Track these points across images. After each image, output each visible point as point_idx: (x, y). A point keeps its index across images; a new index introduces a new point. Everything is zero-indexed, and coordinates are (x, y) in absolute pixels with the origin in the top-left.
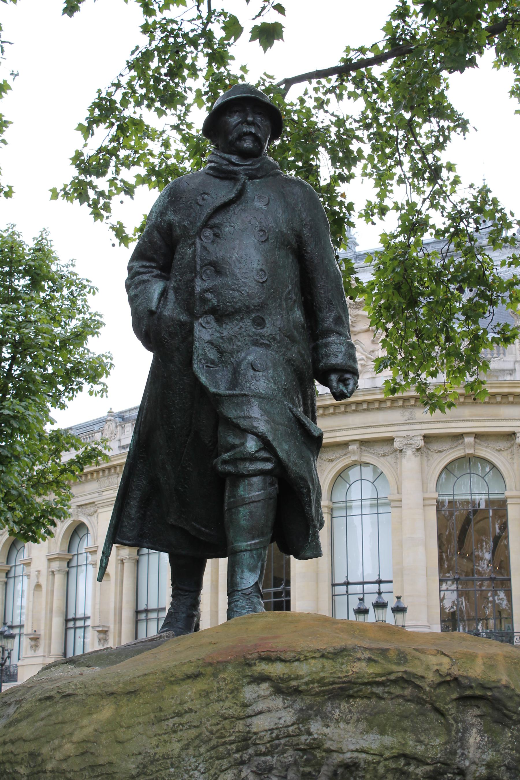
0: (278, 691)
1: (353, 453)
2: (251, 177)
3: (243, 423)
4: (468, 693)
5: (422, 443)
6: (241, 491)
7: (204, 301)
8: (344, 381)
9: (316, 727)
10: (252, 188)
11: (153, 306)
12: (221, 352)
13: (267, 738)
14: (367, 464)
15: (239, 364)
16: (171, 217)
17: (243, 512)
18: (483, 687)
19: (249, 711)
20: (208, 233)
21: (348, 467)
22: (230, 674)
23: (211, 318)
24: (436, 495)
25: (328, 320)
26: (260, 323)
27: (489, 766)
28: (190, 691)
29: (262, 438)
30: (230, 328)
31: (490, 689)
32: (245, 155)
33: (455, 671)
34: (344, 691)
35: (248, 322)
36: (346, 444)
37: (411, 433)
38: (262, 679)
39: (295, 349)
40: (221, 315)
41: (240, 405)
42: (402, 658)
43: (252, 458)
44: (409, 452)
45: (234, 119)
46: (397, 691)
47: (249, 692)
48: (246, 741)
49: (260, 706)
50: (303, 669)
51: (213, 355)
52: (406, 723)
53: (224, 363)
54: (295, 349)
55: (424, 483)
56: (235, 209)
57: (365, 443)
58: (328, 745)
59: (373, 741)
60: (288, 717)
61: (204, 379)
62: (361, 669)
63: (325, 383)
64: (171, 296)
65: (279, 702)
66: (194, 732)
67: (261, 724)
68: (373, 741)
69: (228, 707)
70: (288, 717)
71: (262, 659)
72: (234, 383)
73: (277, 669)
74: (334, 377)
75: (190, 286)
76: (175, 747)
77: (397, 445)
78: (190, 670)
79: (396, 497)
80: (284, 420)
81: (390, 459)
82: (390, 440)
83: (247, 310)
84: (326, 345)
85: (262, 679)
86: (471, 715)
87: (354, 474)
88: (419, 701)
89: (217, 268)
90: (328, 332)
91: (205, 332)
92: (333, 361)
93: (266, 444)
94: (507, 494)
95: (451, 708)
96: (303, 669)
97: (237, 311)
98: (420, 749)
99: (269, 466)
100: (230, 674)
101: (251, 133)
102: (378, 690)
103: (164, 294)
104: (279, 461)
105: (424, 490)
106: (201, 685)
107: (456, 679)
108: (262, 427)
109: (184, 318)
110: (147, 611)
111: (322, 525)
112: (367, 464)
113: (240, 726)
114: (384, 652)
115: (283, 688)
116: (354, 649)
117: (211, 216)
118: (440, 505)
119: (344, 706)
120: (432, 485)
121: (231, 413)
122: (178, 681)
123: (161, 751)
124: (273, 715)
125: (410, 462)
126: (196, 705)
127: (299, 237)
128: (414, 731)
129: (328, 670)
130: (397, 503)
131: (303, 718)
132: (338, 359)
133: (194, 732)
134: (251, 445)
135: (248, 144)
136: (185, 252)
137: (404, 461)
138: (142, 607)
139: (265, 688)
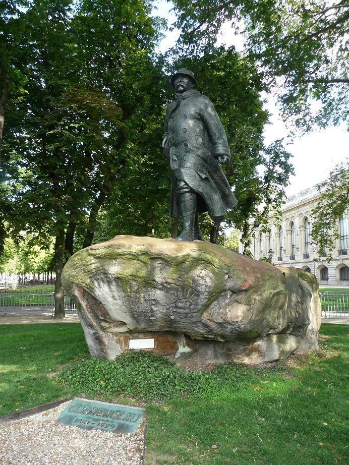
4: (153, 257)
13: (95, 271)
19: (89, 263)
31: (160, 255)
39: (200, 151)
46: (127, 256)
54: (200, 151)
56: (177, 111)
58: (110, 272)
73: (93, 252)
86: (158, 263)
92: (218, 152)
93: (186, 184)
104: (191, 188)
116: (115, 245)
126: (77, 262)
127: (200, 115)
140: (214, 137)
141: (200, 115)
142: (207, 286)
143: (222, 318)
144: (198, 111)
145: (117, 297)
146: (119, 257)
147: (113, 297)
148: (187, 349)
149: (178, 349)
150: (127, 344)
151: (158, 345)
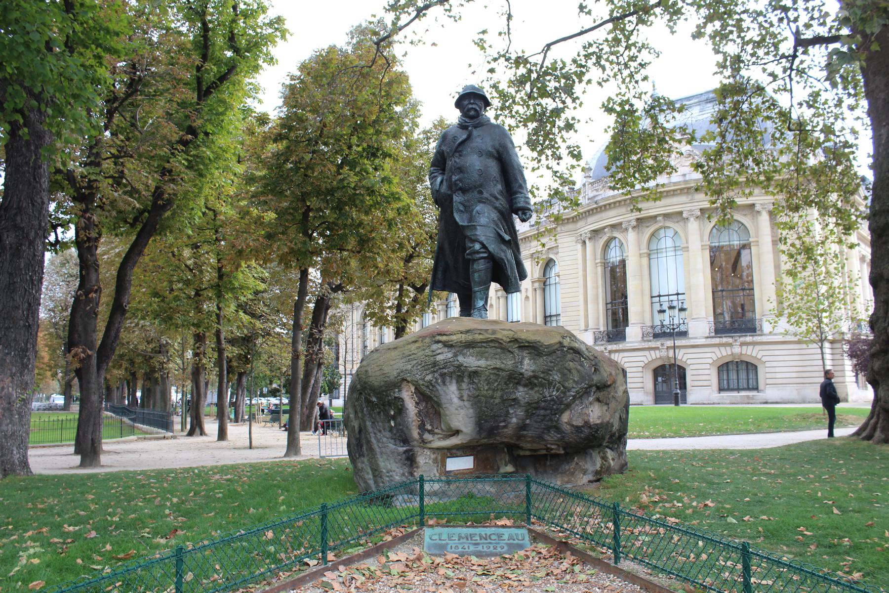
0: (445, 346)
1: (660, 221)
2: (475, 127)
3: (473, 237)
5: (699, 213)
6: (475, 266)
7: (456, 185)
8: (525, 214)
9: (461, 359)
10: (475, 133)
11: (437, 188)
12: (465, 207)
14: (669, 227)
15: (472, 211)
16: (444, 148)
17: (476, 275)
18: (528, 342)
20: (457, 154)
21: (657, 230)
22: (427, 340)
23: (460, 192)
24: (709, 243)
25: (515, 186)
26: (481, 193)
27: (533, 371)
28: (413, 347)
29: (482, 243)
30: (469, 196)
32: (472, 118)
33: (516, 336)
34: (470, 345)
35: (476, 192)
36: (656, 217)
37: (693, 208)
38: (439, 342)
40: (464, 191)
41: (472, 230)
42: (494, 332)
43: (478, 252)
44: (692, 219)
45: (466, 102)
46: (493, 345)
47: (435, 347)
48: (435, 364)
49: (439, 351)
50: (454, 337)
51: (462, 208)
52: (497, 356)
53: (466, 211)
55: (702, 236)
57: (666, 216)
58: (465, 365)
59: (482, 363)
60: (450, 355)
61: (457, 219)
62: (478, 337)
63: (517, 214)
64: (444, 183)
65: (446, 350)
66: (415, 362)
67: (440, 358)
68: (482, 363)
69: (428, 352)
70: (450, 355)
71: (439, 335)
72: (471, 219)
73: (444, 338)
74: (520, 213)
75: (450, 178)
76: (409, 367)
77: (684, 215)
78: (414, 339)
79: (685, 245)
80: (492, 235)
81: (682, 224)
82: (681, 213)
83: (475, 188)
84: (516, 198)
85: (439, 342)
87: (662, 232)
88: (502, 348)
89: (460, 170)
90: (516, 193)
91: (457, 198)
92: (519, 205)
93: (484, 246)
94: (751, 240)
95: (516, 351)
96: (454, 337)
97: (470, 188)
98: (503, 366)
99: (485, 255)
100: (427, 340)
101: (472, 108)
102: (484, 345)
103: (442, 182)
104: (489, 252)
105: (702, 241)
106: (417, 345)
107: (516, 340)
108: (482, 239)
109: (449, 192)
110: (550, 316)
111: (523, 276)
112: (669, 227)
113: (432, 359)
114: (486, 330)
115: (446, 345)
117: (457, 148)
118: (713, 250)
119: (471, 350)
120: (706, 237)
121: (469, 233)
122: (409, 344)
123: (404, 368)
124: (445, 355)
125: (693, 226)
128: (500, 359)
129: (463, 337)
130: (686, 249)
131: (455, 355)
132: (521, 204)
133: (415, 362)
134: (477, 246)
135: (472, 113)
136: (449, 163)
137: (689, 224)
138: (548, 314)
139: (440, 345)
140: (514, 185)
141: (498, 152)
142: (574, 381)
143: (583, 420)
144: (497, 146)
145: (465, 398)
146: (480, 345)
147: (461, 398)
148: (510, 468)
149: (498, 469)
150: (444, 464)
151: (478, 465)
